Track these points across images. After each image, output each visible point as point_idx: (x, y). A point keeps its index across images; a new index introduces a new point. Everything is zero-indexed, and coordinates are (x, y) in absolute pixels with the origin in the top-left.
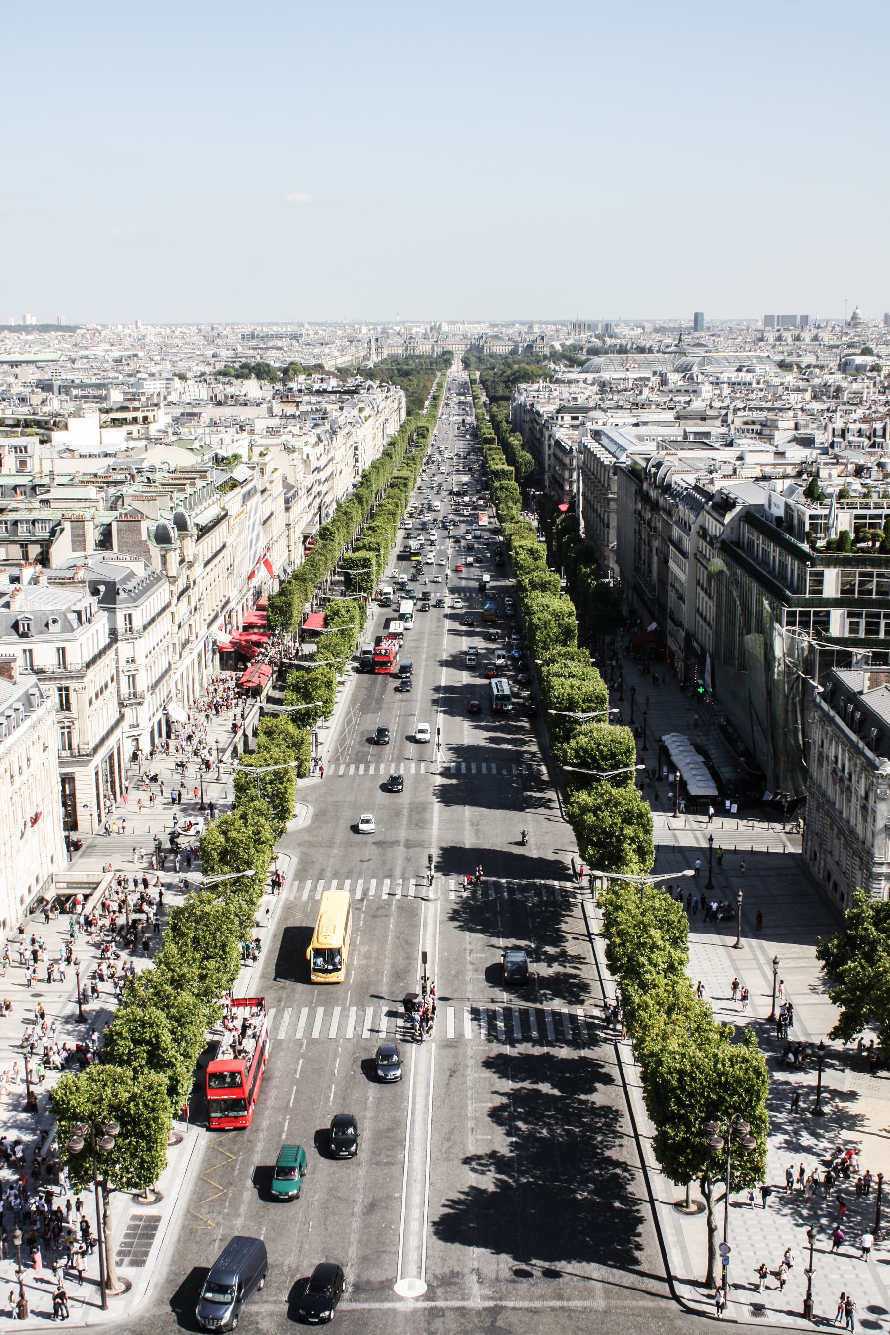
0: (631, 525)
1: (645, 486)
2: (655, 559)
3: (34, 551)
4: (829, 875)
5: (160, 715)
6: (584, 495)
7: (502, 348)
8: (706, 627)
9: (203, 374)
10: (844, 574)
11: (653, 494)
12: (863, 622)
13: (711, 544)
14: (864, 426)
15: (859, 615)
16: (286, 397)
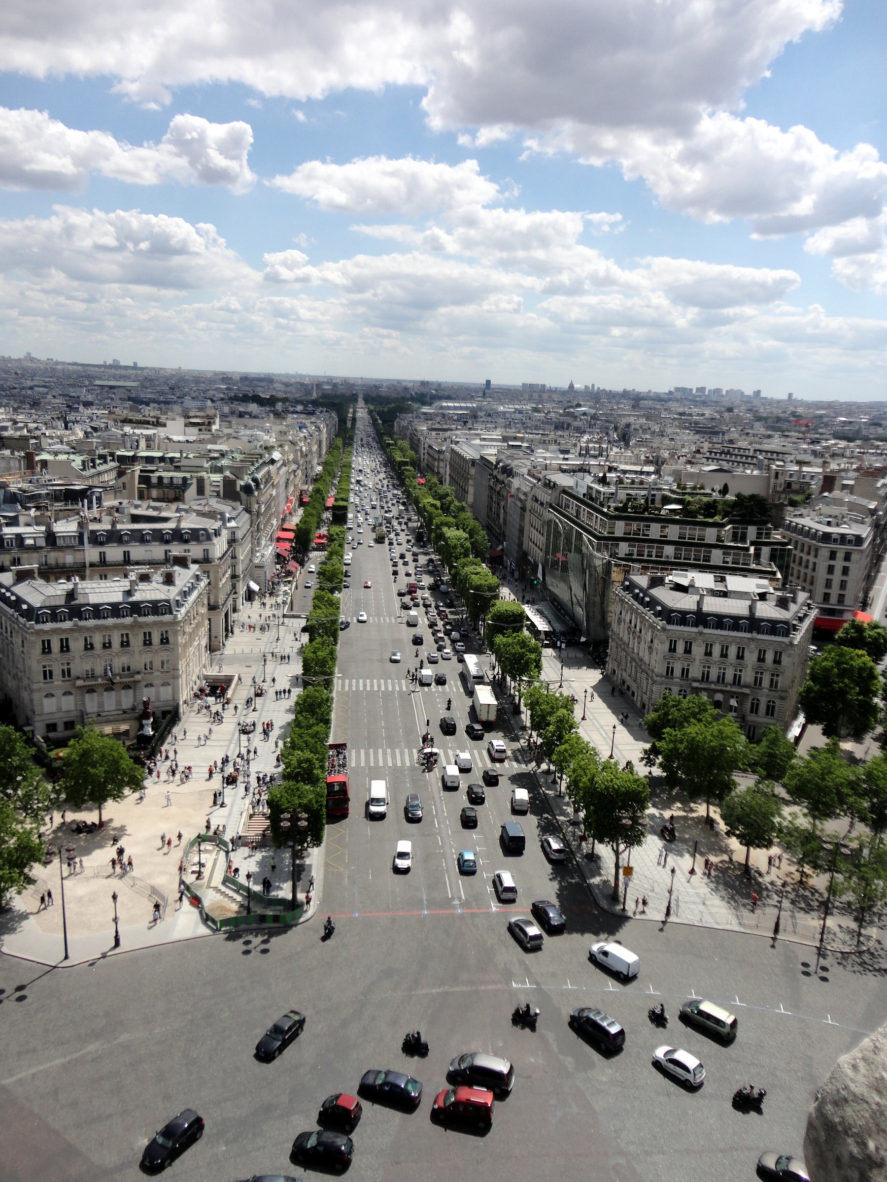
0: (485, 493)
1: (495, 473)
3: (171, 494)
4: (624, 682)
7: (384, 394)
8: (536, 549)
9: (222, 399)
10: (626, 525)
11: (501, 477)
12: (636, 550)
13: (542, 504)
16: (277, 415)
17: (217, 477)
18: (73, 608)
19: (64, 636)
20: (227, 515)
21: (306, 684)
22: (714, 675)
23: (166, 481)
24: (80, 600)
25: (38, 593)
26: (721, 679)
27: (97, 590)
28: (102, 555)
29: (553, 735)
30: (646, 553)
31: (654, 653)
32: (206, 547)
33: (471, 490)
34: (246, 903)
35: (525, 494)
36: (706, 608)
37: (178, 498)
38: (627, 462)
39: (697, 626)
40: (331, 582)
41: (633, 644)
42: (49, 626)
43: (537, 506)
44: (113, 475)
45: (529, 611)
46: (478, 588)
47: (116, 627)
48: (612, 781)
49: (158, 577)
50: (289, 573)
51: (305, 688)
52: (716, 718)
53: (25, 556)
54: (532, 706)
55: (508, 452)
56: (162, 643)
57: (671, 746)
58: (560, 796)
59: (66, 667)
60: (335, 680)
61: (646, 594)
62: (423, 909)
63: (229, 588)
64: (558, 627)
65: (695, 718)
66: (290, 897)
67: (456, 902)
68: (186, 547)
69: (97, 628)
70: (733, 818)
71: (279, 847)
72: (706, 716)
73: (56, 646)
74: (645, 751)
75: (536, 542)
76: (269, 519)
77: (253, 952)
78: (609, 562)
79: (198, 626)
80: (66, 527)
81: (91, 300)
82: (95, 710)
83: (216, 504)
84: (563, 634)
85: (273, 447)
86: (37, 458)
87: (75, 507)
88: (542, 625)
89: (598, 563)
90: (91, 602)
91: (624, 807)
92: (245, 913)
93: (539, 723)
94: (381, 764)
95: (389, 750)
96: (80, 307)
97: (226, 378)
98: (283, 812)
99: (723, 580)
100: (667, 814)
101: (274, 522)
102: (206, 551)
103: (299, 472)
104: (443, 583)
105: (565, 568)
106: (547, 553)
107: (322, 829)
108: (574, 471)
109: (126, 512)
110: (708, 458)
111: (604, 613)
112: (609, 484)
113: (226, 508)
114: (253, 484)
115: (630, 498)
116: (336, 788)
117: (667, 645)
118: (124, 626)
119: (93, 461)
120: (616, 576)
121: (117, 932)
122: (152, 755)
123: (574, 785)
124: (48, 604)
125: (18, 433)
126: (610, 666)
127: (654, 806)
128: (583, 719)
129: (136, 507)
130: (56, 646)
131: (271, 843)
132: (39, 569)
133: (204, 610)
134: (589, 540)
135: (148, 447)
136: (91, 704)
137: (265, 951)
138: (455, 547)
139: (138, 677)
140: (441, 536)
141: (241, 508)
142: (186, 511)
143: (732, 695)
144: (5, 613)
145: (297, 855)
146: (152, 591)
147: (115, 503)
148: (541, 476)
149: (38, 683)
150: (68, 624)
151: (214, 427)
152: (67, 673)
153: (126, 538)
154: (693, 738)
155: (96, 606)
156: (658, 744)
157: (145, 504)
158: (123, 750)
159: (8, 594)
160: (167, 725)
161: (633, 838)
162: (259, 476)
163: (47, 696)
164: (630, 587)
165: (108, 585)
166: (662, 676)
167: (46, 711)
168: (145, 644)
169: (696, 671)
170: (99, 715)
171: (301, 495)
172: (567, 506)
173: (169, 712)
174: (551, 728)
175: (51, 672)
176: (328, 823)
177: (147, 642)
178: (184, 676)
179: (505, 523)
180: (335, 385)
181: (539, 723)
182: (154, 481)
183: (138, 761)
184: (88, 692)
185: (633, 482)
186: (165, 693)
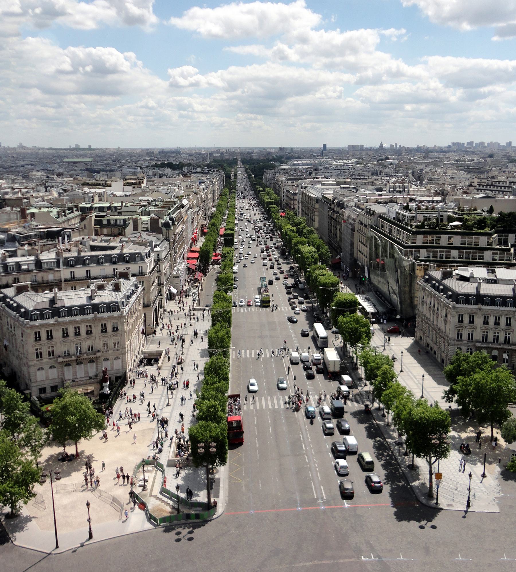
1: (332, 206)
2: (338, 232)
3: (116, 231)
4: (428, 345)
5: (168, 291)
6: (302, 209)
7: (254, 158)
9: (148, 167)
11: (336, 209)
12: (431, 254)
13: (365, 226)
14: (401, 185)
15: (430, 252)
16: (184, 175)
17: (146, 218)
18: (55, 310)
19: (49, 329)
20: (154, 243)
21: (211, 355)
22: (491, 337)
23: (112, 222)
24: (59, 304)
25: (31, 301)
26: (496, 340)
27: (70, 297)
28: (72, 273)
29: (380, 383)
30: (439, 256)
31: (448, 324)
32: (140, 265)
33: (317, 219)
34: (176, 506)
35: (354, 220)
36: (482, 292)
37: (120, 234)
38: (422, 194)
39: (477, 304)
40: (226, 285)
41: (433, 318)
42: (39, 322)
43: (362, 227)
44: (78, 220)
45: (360, 299)
46: (324, 285)
47: (82, 321)
48: (423, 413)
49: (109, 287)
50: (196, 280)
51: (210, 357)
52: (493, 367)
53: (22, 276)
54: (365, 364)
55: (341, 192)
56: (114, 330)
57: (464, 388)
58: (388, 425)
59: (51, 350)
60: (231, 351)
61: (440, 284)
62: (297, 507)
63: (157, 292)
64: (381, 309)
65: (479, 368)
66: (206, 500)
67: (320, 501)
68: (127, 265)
69: (70, 322)
70: (510, 437)
71: (197, 467)
72: (487, 366)
73: (44, 336)
74: (446, 392)
75: (362, 252)
76: (182, 244)
77: (183, 539)
78: (414, 263)
79: (137, 318)
80: (48, 256)
81: (58, 106)
82: (71, 378)
83: (146, 236)
84: (384, 313)
85: (183, 196)
86: (28, 212)
87: (54, 242)
88: (369, 308)
89: (406, 264)
90: (66, 305)
91: (433, 432)
92: (176, 513)
93: (371, 375)
94: (264, 407)
95: (269, 398)
96: (51, 112)
97: (149, 153)
98: (199, 442)
99: (493, 272)
100: (464, 435)
101: (186, 247)
102: (141, 268)
103: (201, 213)
104: (300, 283)
105: (383, 269)
106: (370, 259)
107: (226, 453)
108: (386, 203)
109: (87, 245)
110: (478, 190)
111: (412, 299)
112: (411, 210)
113: (153, 239)
114: (170, 221)
115: (426, 219)
116: (235, 425)
117: (457, 319)
118: (88, 320)
119: (64, 211)
120: (419, 272)
121: (90, 528)
122: (110, 406)
123: (397, 418)
124: (38, 308)
125: (15, 196)
126: (418, 334)
127: (454, 430)
128: (401, 371)
129: (94, 240)
130: (44, 336)
131: (191, 464)
132: (31, 284)
133: (141, 308)
134: (399, 249)
135: (100, 200)
136: (68, 373)
137: (190, 539)
138: (308, 258)
139: (98, 354)
140: (298, 251)
141: (163, 238)
142: (127, 242)
143: (504, 351)
144: (10, 315)
145: (209, 472)
146: (106, 296)
147: (80, 238)
148: (364, 207)
149: (33, 360)
150: (51, 321)
151: (143, 185)
152: (51, 354)
153: (88, 261)
154: (479, 383)
155: (70, 308)
156: (454, 387)
157: (99, 238)
158: (90, 404)
159: (11, 302)
160: (119, 386)
161: (441, 452)
162: (174, 216)
163: (39, 369)
164: (429, 280)
165: (77, 293)
166: (454, 340)
167: (38, 380)
168: (102, 332)
169: (478, 336)
170: (74, 381)
171: (202, 227)
172: (383, 226)
173: (120, 377)
174: (379, 378)
175: (41, 354)
176: (229, 449)
177: (104, 330)
178: (129, 353)
179: (341, 240)
180: (222, 153)
181: (370, 375)
182: (105, 222)
183: (99, 410)
184: (66, 365)
185: (427, 208)
186: (117, 365)
